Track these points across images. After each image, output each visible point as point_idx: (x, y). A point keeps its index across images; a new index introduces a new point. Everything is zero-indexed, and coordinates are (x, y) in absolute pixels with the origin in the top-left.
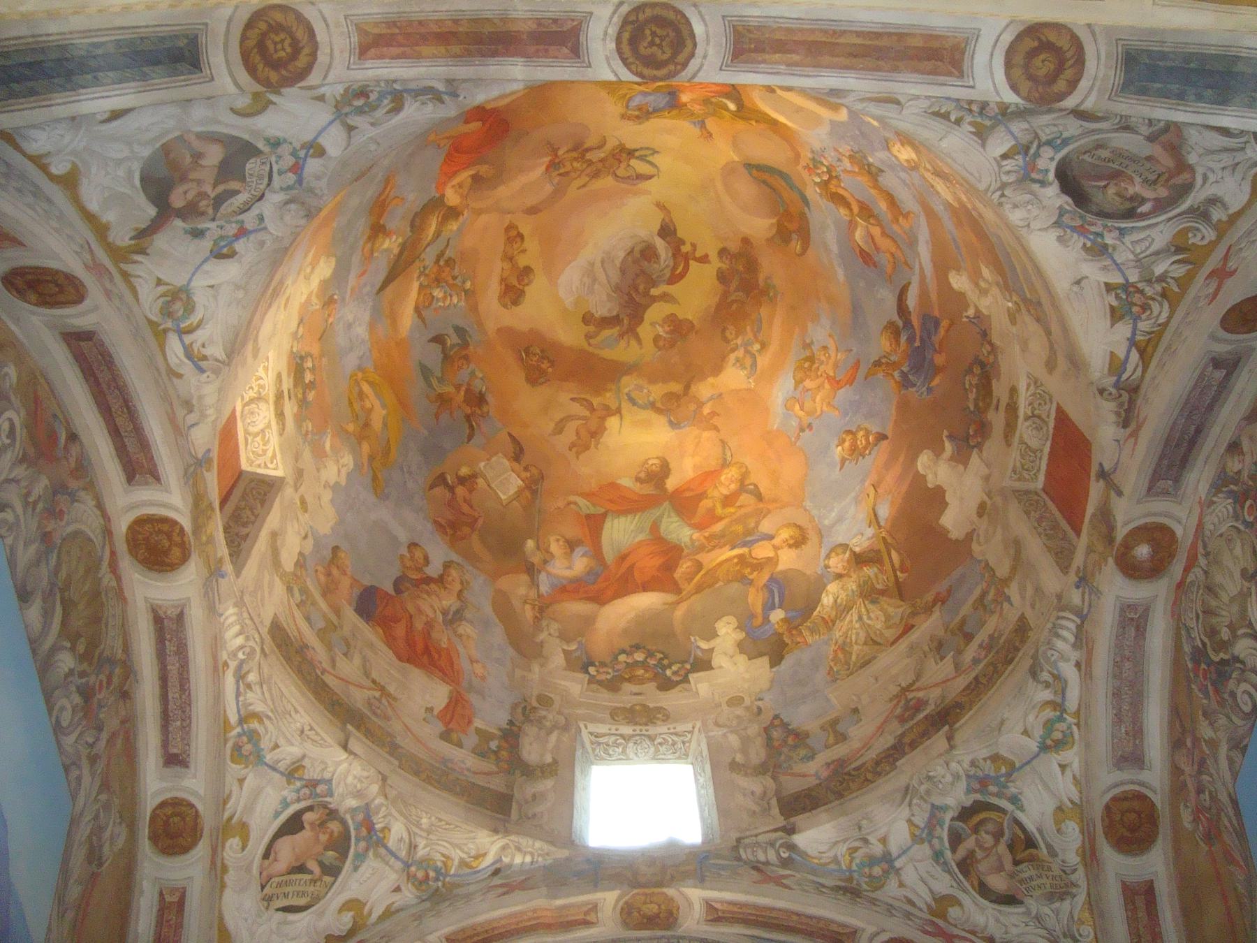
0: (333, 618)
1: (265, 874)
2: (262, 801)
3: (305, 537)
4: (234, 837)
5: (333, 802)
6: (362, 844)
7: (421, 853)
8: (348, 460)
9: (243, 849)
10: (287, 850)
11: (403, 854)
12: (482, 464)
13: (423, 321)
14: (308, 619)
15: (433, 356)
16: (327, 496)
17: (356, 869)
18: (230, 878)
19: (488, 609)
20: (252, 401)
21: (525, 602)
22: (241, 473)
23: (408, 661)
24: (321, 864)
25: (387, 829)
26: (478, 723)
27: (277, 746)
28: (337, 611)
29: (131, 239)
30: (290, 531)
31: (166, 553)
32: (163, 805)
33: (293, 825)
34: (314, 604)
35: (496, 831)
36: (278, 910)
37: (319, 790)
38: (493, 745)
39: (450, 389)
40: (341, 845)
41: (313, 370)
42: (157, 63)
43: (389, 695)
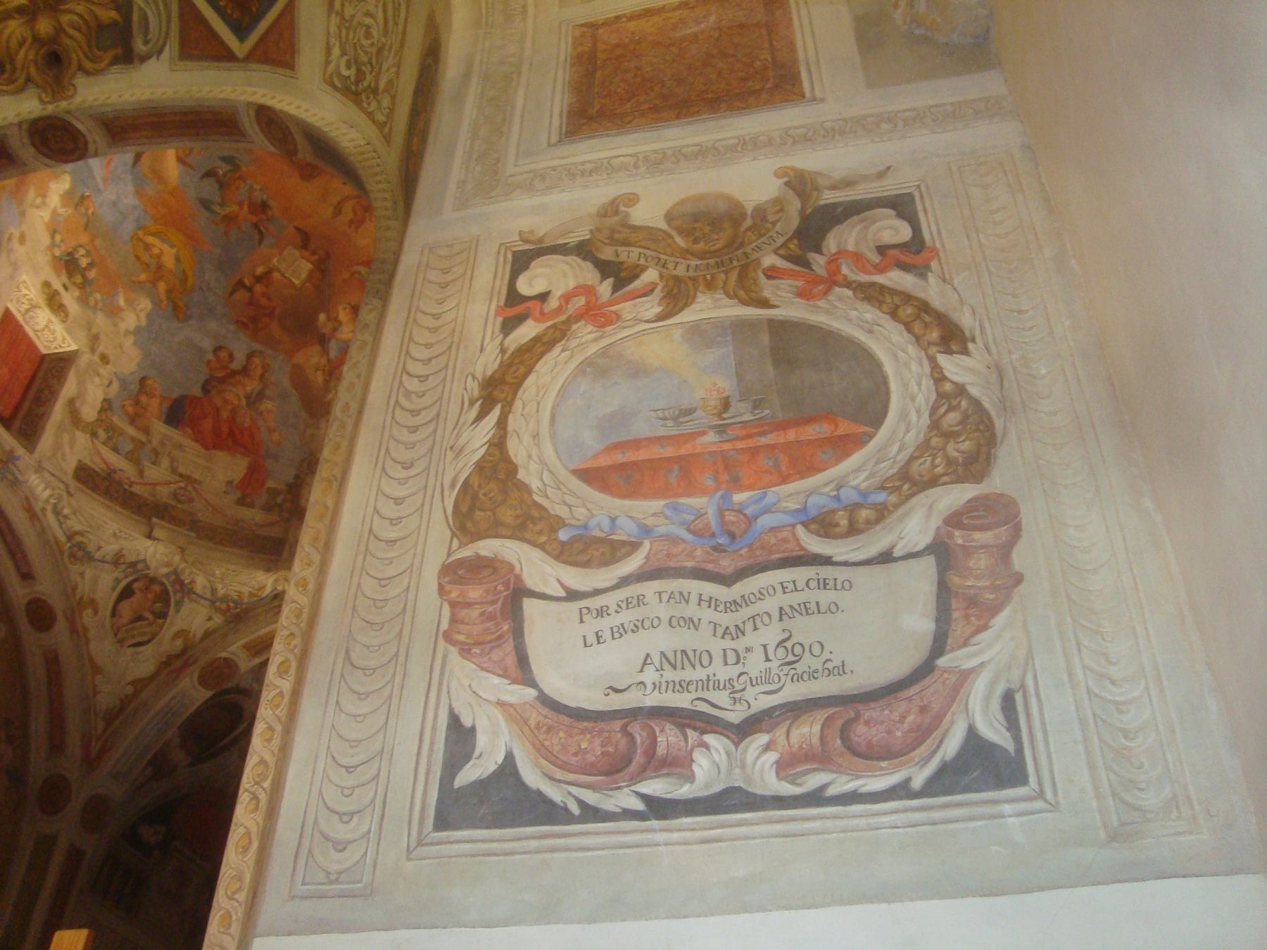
0: (142, 437)
2: (101, 584)
3: (110, 383)
5: (151, 573)
6: (179, 595)
7: (221, 592)
8: (145, 304)
10: (126, 609)
11: (208, 596)
12: (275, 261)
13: (191, 167)
14: (115, 450)
15: (209, 189)
16: (129, 341)
17: (178, 611)
19: (287, 384)
20: (27, 311)
21: (317, 370)
22: (44, 357)
23: (214, 447)
24: (153, 612)
25: (193, 582)
26: (270, 484)
27: (100, 548)
28: (146, 431)
30: (87, 391)
32: (30, 603)
33: (127, 593)
34: (122, 433)
35: (268, 570)
37: (140, 566)
38: (279, 500)
39: (232, 209)
40: (164, 597)
41: (88, 254)
43: (195, 481)
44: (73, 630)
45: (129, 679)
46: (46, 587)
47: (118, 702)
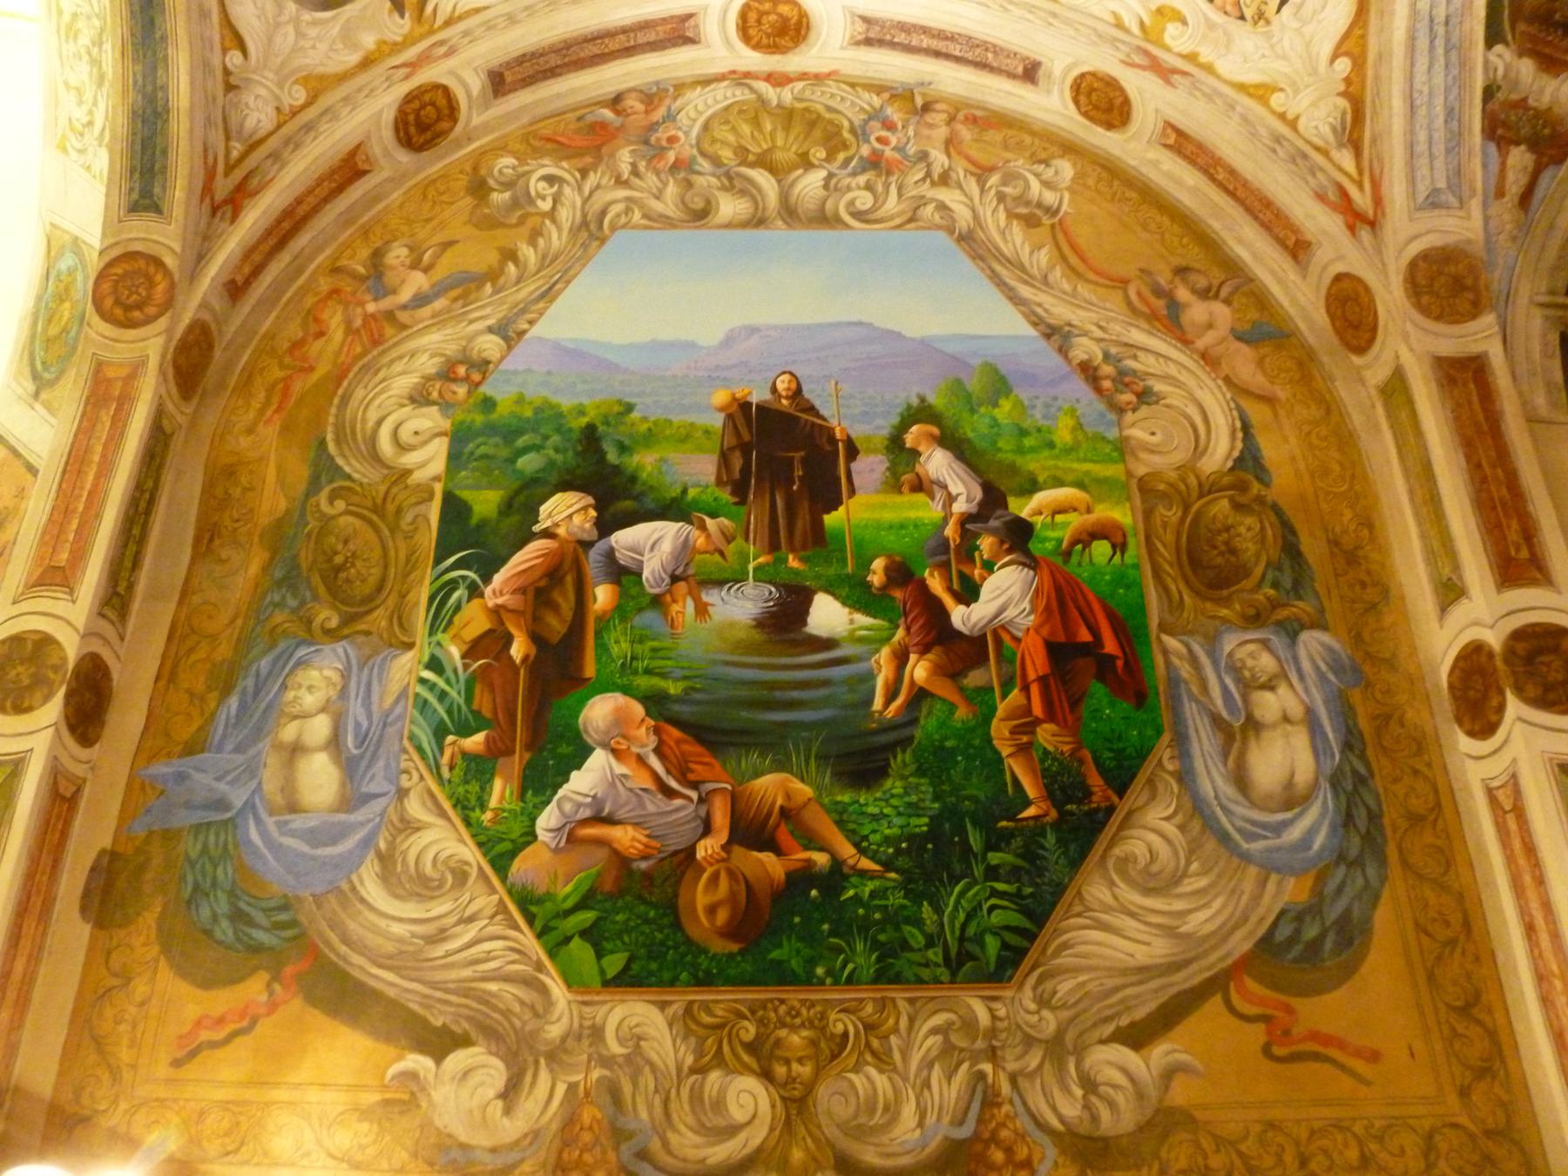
1: (1229, 8)
4: (1163, 30)
9: (1184, 22)
18: (1206, 55)
29: (402, 16)
31: (785, 20)
32: (1076, 102)
36: (1279, 10)
42: (152, 22)
44: (1165, 73)
45: (1327, 49)
46: (1066, 56)
47: (1343, 103)
